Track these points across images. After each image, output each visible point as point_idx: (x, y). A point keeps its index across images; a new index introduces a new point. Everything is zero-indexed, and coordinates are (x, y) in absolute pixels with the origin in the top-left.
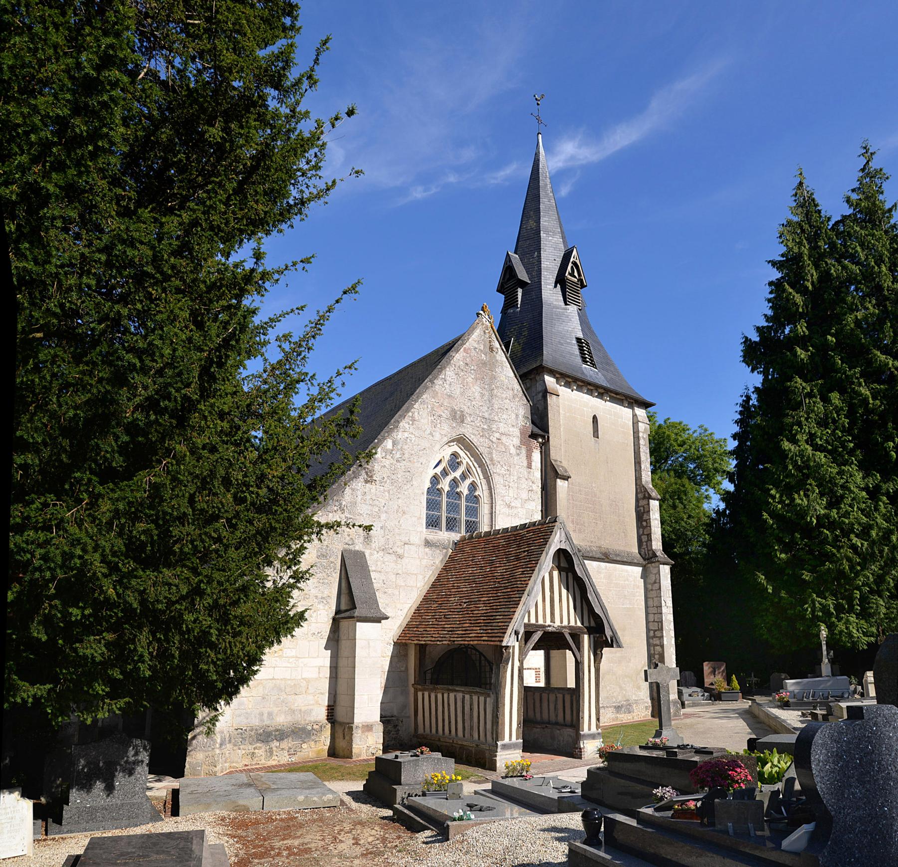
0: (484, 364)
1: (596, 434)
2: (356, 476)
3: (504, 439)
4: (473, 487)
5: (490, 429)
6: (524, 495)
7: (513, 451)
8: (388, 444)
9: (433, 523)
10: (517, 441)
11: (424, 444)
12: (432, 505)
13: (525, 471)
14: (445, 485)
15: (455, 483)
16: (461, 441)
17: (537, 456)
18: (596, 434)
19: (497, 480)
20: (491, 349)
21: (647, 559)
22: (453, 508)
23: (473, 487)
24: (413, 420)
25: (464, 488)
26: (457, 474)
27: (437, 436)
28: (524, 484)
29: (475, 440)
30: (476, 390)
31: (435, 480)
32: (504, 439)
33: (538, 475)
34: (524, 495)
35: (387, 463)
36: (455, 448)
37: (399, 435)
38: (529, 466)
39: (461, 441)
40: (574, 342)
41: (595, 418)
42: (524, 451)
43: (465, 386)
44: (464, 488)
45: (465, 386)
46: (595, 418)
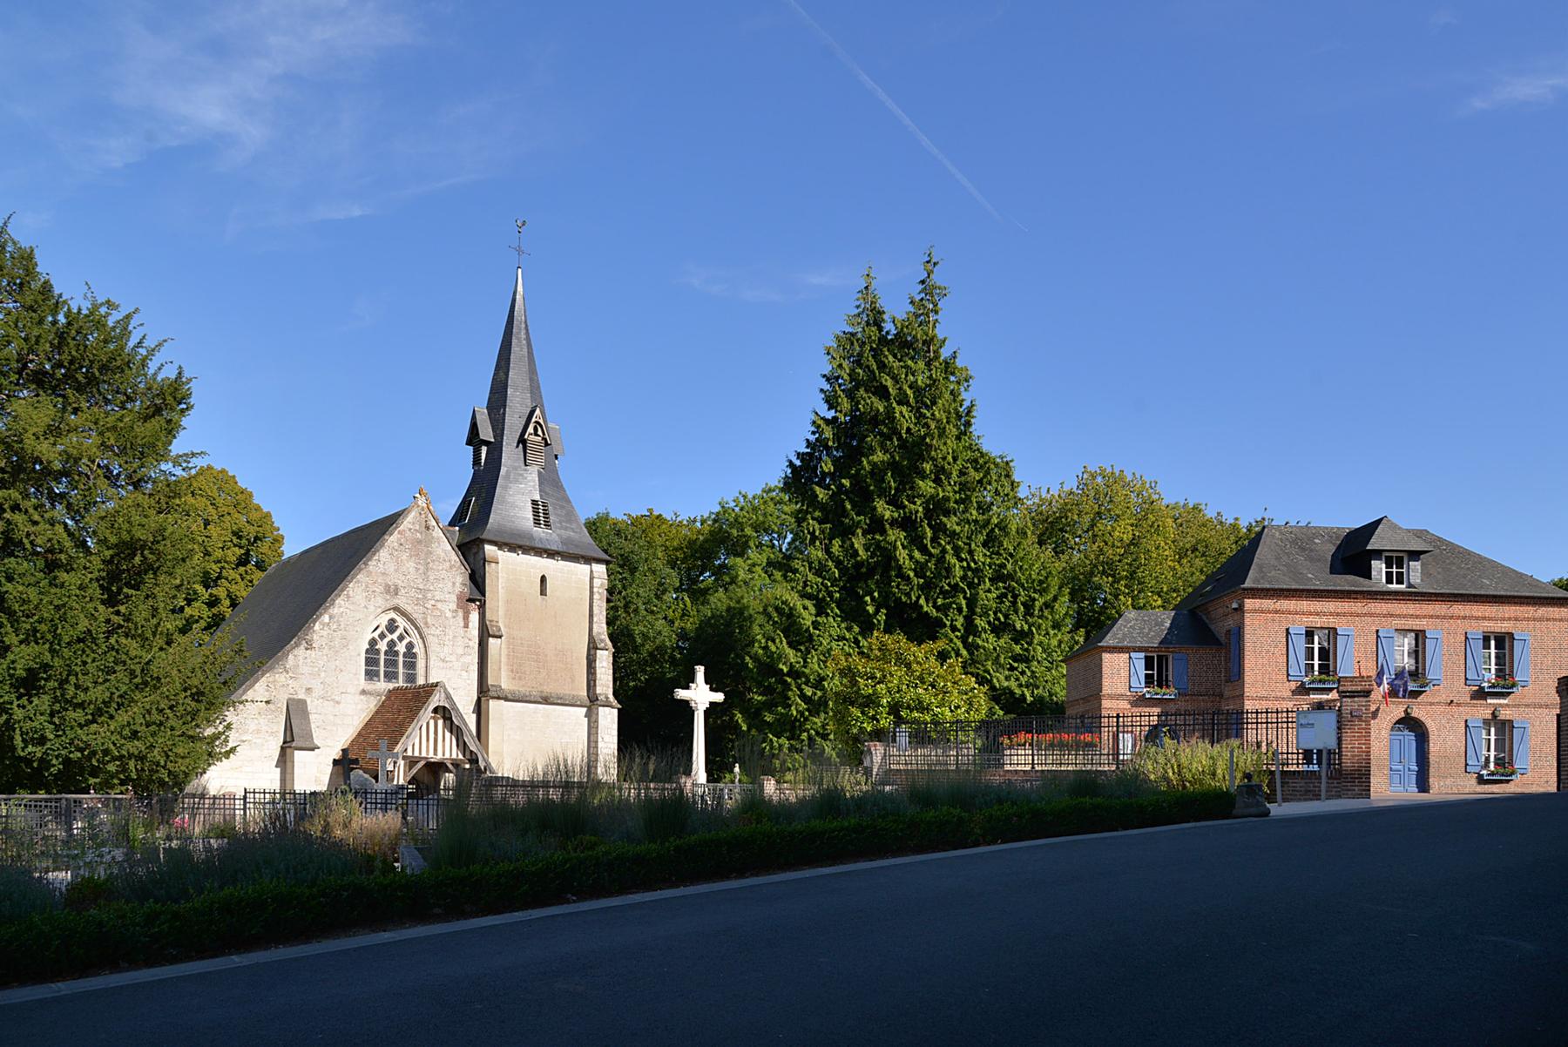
0: (420, 542)
1: (543, 592)
2: (297, 645)
3: (439, 605)
4: (410, 646)
5: (425, 597)
6: (460, 651)
7: (449, 614)
8: (326, 618)
9: (371, 675)
10: (454, 606)
11: (359, 616)
12: (371, 661)
13: (461, 631)
14: (382, 646)
15: (392, 644)
16: (396, 609)
17: (474, 617)
18: (543, 592)
19: (430, 639)
20: (428, 528)
21: (593, 702)
22: (392, 663)
23: (410, 646)
24: (348, 597)
25: (401, 648)
26: (395, 636)
27: (372, 608)
28: (460, 642)
29: (409, 609)
30: (411, 565)
31: (373, 642)
32: (439, 605)
33: (476, 633)
34: (460, 651)
35: (324, 633)
36: (392, 615)
37: (335, 610)
38: (466, 626)
39: (396, 609)
40: (529, 505)
41: (543, 579)
42: (461, 614)
43: (399, 563)
44: (401, 648)
45: (399, 563)
46: (543, 579)
